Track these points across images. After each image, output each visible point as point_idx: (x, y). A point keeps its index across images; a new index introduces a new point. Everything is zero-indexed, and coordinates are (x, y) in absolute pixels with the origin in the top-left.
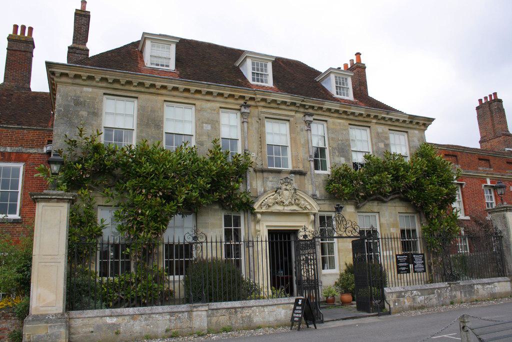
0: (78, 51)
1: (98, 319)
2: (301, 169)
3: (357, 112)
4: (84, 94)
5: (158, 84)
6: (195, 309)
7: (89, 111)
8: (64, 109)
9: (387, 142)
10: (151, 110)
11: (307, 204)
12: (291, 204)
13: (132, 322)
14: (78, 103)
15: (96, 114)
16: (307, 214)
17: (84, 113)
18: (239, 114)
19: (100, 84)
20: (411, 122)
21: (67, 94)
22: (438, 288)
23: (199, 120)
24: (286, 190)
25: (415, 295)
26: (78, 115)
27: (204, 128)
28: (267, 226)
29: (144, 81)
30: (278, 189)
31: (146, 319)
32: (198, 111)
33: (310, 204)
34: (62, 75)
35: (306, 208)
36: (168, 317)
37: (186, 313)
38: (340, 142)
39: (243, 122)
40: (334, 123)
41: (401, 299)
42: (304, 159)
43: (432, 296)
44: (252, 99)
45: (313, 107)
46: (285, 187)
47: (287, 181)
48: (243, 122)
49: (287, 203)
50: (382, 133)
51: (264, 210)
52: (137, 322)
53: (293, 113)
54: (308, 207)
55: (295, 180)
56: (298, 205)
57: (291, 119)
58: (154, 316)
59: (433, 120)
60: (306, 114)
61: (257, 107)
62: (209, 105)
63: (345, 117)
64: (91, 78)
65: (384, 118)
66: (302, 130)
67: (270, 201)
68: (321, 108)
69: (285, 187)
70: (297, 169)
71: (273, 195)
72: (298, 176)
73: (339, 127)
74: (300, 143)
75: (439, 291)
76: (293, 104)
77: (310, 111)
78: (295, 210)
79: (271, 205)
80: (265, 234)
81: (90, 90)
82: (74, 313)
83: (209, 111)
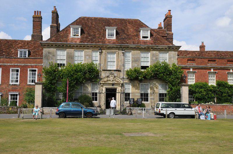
0: (53, 27)
12: (113, 81)
14: (49, 53)
16: (119, 84)
17: (51, 56)
18: (98, 52)
19: (55, 47)
30: (108, 76)
33: (120, 81)
35: (118, 82)
47: (112, 74)
49: (111, 80)
51: (103, 82)
54: (119, 82)
55: (116, 74)
57: (117, 52)
59: (180, 47)
62: (88, 50)
63: (139, 49)
65: (156, 48)
66: (121, 56)
70: (117, 69)
77: (124, 48)
80: (104, 90)
82: (43, 108)
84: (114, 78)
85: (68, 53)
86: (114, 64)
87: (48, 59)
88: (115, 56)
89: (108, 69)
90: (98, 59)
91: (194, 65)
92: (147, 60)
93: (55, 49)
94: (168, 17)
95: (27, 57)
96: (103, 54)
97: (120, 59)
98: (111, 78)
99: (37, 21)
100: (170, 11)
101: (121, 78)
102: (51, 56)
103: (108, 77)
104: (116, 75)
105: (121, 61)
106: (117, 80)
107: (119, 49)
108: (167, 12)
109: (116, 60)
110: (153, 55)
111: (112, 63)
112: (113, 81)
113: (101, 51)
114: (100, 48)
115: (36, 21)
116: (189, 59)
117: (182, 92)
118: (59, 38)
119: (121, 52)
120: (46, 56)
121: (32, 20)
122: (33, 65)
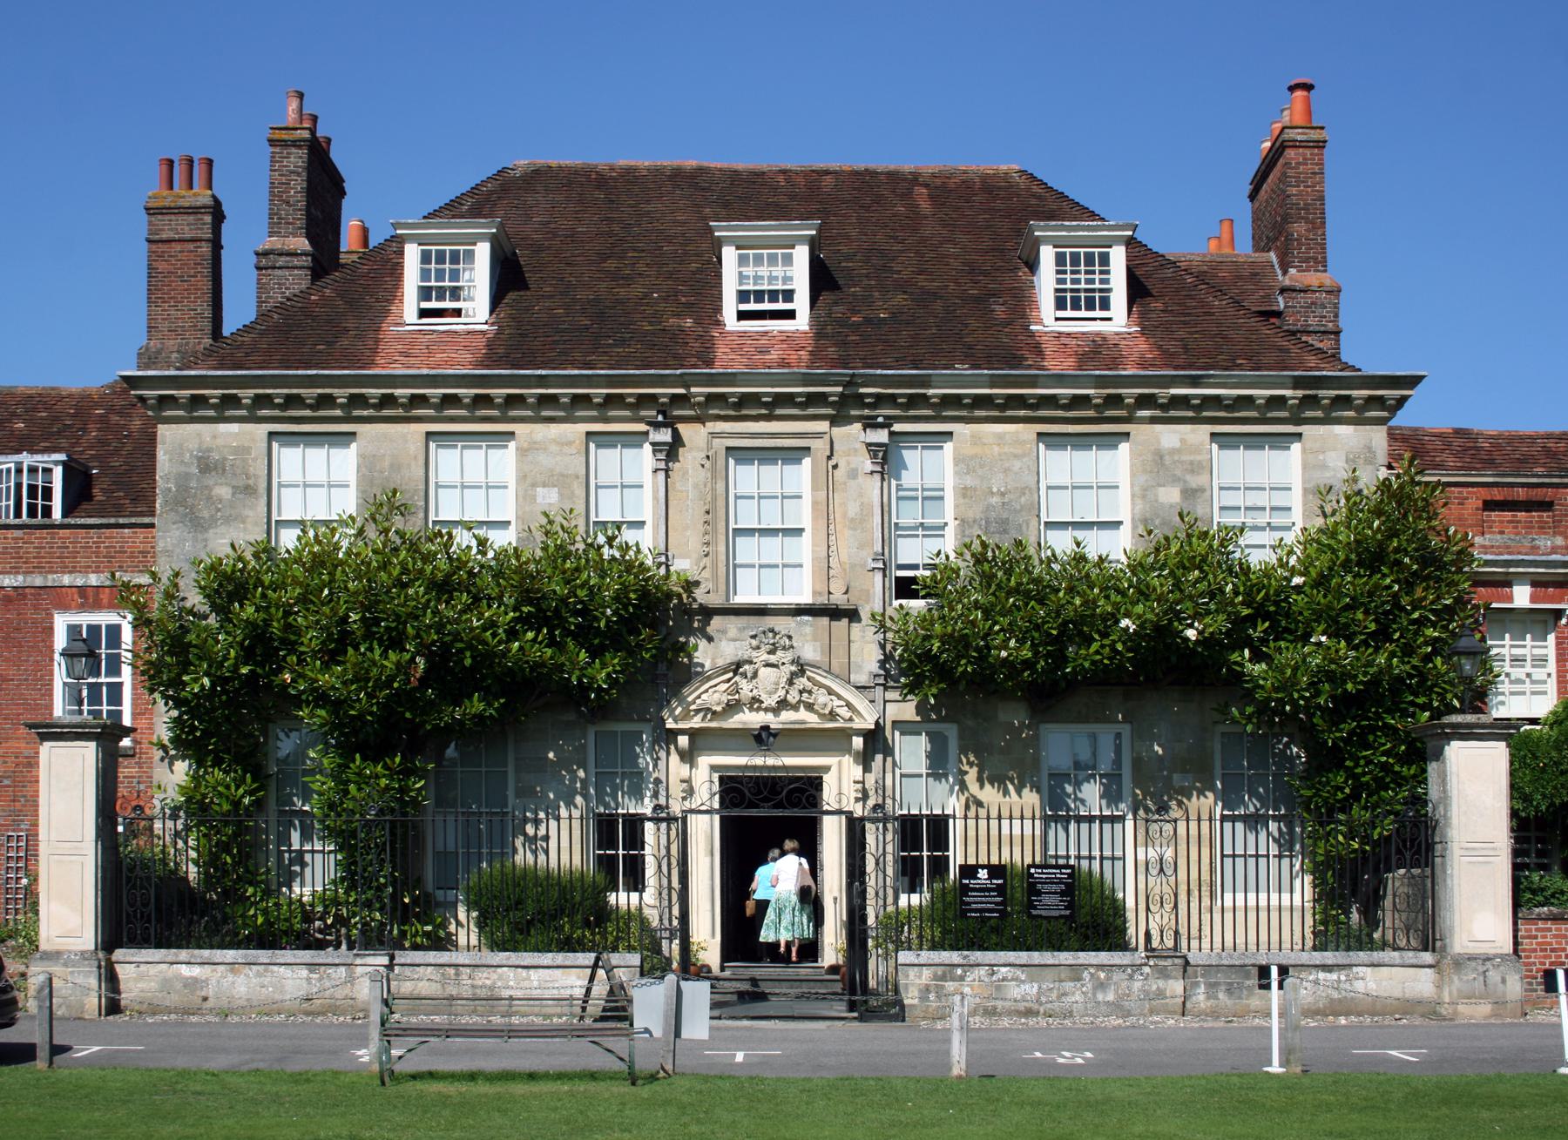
0: (282, 261)
1: (164, 966)
2: (838, 599)
4: (220, 442)
6: (358, 961)
7: (234, 483)
8: (178, 486)
9: (1194, 481)
10: (392, 465)
11: (837, 702)
12: (783, 704)
13: (230, 978)
14: (207, 465)
16: (847, 734)
17: (224, 492)
18: (647, 448)
21: (181, 446)
22: (1100, 967)
23: (525, 477)
24: (768, 665)
25: (1004, 979)
26: (209, 498)
27: (539, 500)
28: (714, 768)
29: (364, 391)
31: (259, 975)
32: (522, 452)
33: (849, 705)
34: (162, 400)
35: (832, 715)
36: (304, 972)
37: (343, 969)
38: (995, 500)
39: (656, 471)
40: (976, 440)
41: (950, 986)
42: (853, 566)
43: (1069, 985)
44: (675, 398)
45: (892, 400)
46: (765, 657)
48: (656, 471)
49: (771, 701)
50: (1173, 451)
51: (696, 722)
52: (241, 979)
53: (823, 426)
55: (808, 640)
56: (810, 707)
58: (275, 968)
60: (870, 424)
61: (700, 420)
62: (555, 430)
64: (231, 401)
65: (1183, 402)
66: (853, 474)
68: (925, 397)
69: (765, 657)
71: (729, 680)
72: (825, 621)
73: (996, 449)
74: (845, 515)
75: (1102, 975)
76: (820, 399)
78: (803, 722)
79: (719, 709)
81: (234, 428)
82: (119, 954)
83: (554, 448)
84: (791, 682)
86: (794, 540)
87: (198, 525)
88: (801, 475)
90: (645, 506)
92: (1096, 501)
94: (1295, 145)
95: (57, 514)
96: (690, 457)
97: (853, 510)
98: (769, 682)
99: (188, 240)
100: (1308, 87)
101: (861, 678)
102: (224, 492)
103: (736, 667)
104: (809, 652)
105: (858, 523)
106: (821, 698)
107: (835, 421)
109: (815, 519)
110: (1157, 466)
111: (771, 548)
112: (783, 704)
113: (665, 436)
114: (664, 413)
115: (171, 235)
116: (1497, 494)
117: (1445, 798)
118: (314, 342)
119: (852, 437)
120: (181, 500)
121: (145, 234)
122: (93, 580)
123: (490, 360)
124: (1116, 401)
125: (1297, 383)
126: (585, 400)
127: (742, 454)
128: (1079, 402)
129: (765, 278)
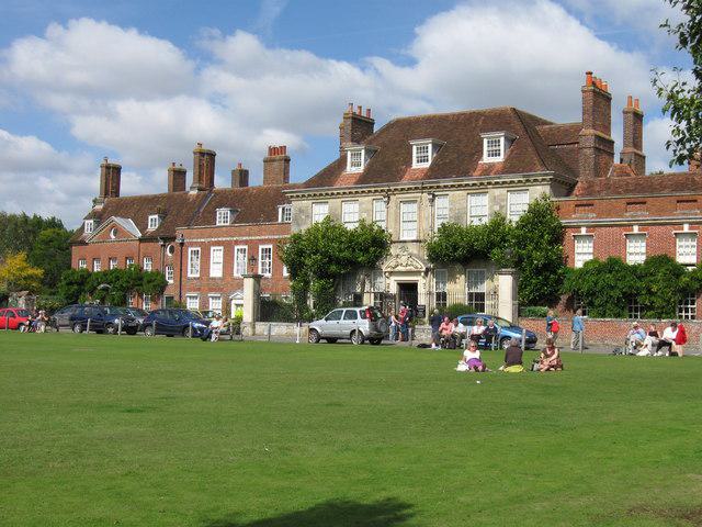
2: (422, 238)
3: (471, 183)
5: (335, 192)
14: (301, 211)
15: (309, 216)
20: (528, 181)
51: (389, 269)
62: (367, 198)
67: (393, 264)
85: (330, 209)
86: (410, 221)
87: (298, 225)
89: (401, 239)
91: (592, 217)
93: (310, 202)
98: (403, 259)
100: (591, 73)
106: (414, 263)
108: (583, 81)
110: (494, 200)
116: (579, 203)
119: (426, 196)
123: (356, 183)
124: (482, 184)
125: (524, 176)
126: (369, 192)
127: (405, 202)
128: (474, 185)
129: (422, 156)
